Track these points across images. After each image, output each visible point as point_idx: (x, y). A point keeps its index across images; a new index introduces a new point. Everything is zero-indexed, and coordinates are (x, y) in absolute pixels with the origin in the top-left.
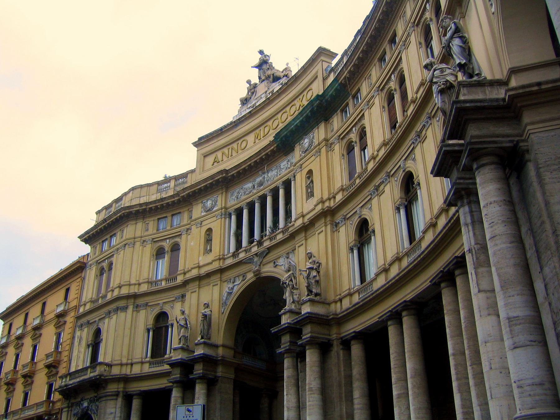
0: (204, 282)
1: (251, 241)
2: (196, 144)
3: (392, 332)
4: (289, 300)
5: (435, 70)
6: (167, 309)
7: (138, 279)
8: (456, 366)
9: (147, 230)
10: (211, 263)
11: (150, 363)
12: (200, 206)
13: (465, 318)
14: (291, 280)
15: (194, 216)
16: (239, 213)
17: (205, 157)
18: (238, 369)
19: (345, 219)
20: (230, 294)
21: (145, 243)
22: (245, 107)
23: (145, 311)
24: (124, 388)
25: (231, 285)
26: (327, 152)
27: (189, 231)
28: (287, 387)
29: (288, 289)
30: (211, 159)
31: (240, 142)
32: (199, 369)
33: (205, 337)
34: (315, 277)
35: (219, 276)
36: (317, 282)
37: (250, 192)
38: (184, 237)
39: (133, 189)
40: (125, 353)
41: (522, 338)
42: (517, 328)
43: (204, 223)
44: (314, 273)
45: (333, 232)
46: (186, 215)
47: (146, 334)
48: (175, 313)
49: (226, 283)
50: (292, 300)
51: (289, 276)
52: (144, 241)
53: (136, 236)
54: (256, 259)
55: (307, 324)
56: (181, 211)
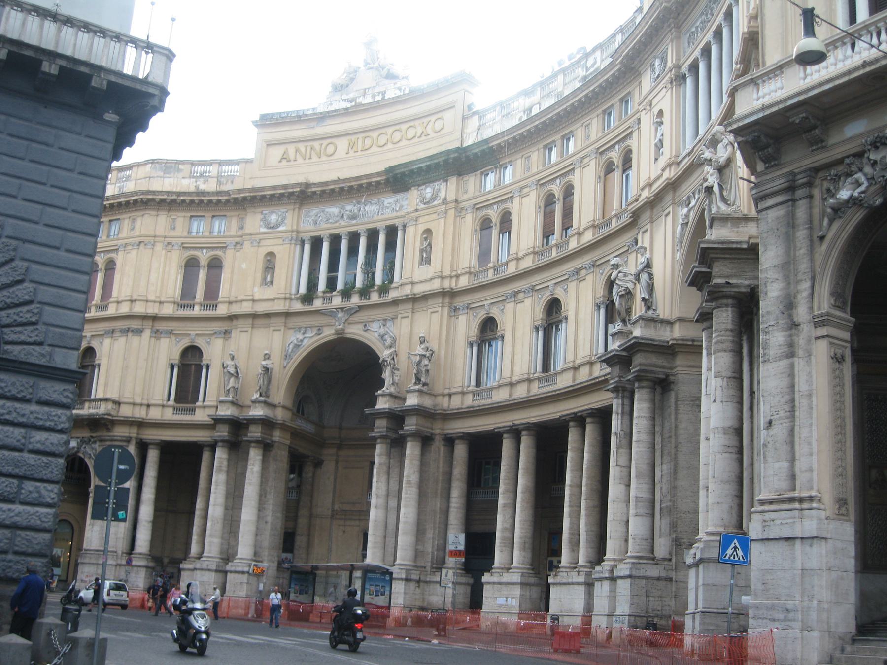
0: (259, 322)
1: (331, 283)
2: (256, 124)
3: (507, 446)
5: (620, 272)
6: (200, 343)
7: (158, 295)
8: (571, 495)
9: (174, 228)
10: (273, 300)
12: (259, 217)
13: (588, 460)
15: (248, 229)
16: (316, 244)
17: (268, 145)
18: (295, 434)
19: (468, 307)
20: (297, 346)
21: (170, 247)
22: (337, 97)
23: (168, 340)
24: (138, 434)
25: (300, 337)
26: (456, 217)
27: (238, 247)
28: (378, 474)
29: (389, 368)
30: (277, 152)
31: (325, 142)
32: (255, 432)
33: (264, 394)
34: (426, 365)
35: (282, 320)
36: (427, 371)
37: (336, 222)
38: (230, 253)
39: (153, 162)
40: (138, 390)
41: (642, 511)
42: (640, 504)
43: (263, 243)
44: (426, 361)
46: (234, 222)
47: (169, 371)
48: (215, 353)
49: (291, 331)
51: (391, 354)
52: (169, 244)
53: (158, 234)
54: (340, 315)
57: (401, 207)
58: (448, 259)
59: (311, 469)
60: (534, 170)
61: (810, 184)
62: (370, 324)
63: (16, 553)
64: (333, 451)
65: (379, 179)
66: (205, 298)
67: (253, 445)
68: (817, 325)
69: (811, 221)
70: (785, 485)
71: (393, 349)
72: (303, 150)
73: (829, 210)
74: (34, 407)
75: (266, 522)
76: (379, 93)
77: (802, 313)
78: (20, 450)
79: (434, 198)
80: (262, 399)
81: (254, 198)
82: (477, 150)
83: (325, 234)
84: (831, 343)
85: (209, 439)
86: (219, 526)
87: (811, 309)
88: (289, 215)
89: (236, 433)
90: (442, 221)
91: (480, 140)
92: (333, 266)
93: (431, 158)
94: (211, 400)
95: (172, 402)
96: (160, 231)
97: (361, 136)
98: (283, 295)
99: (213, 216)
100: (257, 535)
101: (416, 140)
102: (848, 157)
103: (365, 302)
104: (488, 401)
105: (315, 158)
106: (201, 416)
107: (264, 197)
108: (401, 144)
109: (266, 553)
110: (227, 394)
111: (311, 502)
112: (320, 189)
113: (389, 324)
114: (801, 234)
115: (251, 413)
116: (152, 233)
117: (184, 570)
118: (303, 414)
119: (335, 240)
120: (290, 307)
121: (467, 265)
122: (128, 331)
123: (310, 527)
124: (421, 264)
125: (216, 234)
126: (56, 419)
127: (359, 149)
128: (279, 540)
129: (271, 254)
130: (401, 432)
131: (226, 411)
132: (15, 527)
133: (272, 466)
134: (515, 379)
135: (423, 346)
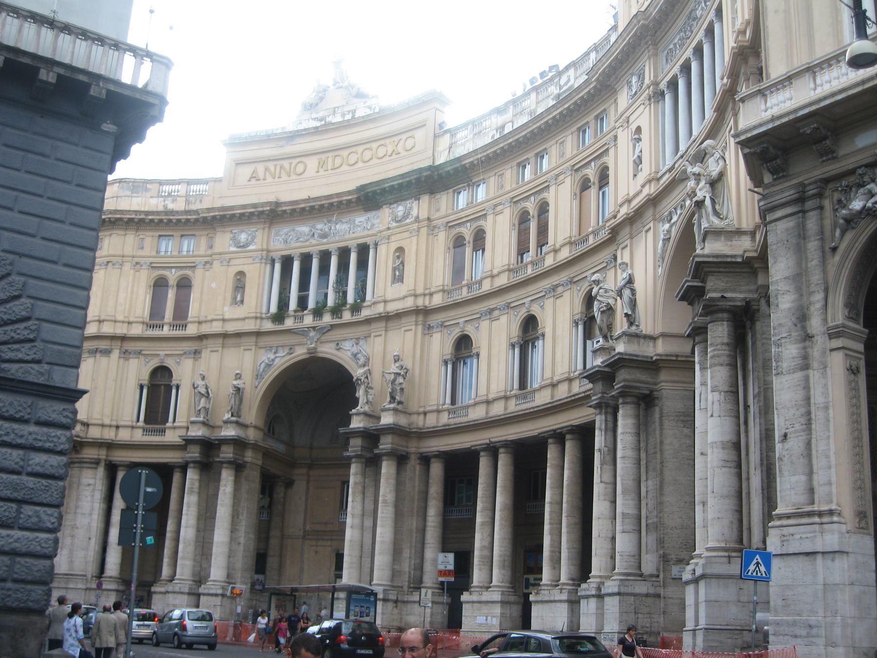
1: (303, 302)
4: (362, 400)
5: (600, 288)
6: (170, 363)
7: (126, 315)
8: (551, 512)
9: (142, 248)
10: (244, 319)
11: (144, 429)
12: (228, 236)
13: (568, 477)
14: (367, 377)
15: (218, 248)
16: (287, 262)
17: (237, 164)
18: (267, 454)
19: (442, 325)
20: (269, 366)
21: (138, 267)
23: (137, 360)
24: (107, 456)
25: (272, 356)
26: (428, 235)
27: (208, 266)
28: (353, 493)
29: (363, 387)
30: (247, 171)
31: (295, 161)
32: (227, 453)
34: (401, 384)
35: (253, 339)
36: (402, 389)
38: (199, 272)
40: (107, 411)
41: (628, 527)
42: (627, 521)
43: (233, 262)
44: (400, 380)
45: (424, 334)
46: (203, 241)
48: (185, 373)
49: (262, 351)
50: (365, 401)
51: (365, 373)
52: (137, 263)
53: (126, 253)
54: (312, 334)
55: (388, 434)
56: (197, 233)
57: (373, 225)
58: (421, 278)
59: (283, 489)
60: (508, 188)
61: (820, 195)
62: (343, 343)
63: (15, 581)
64: (304, 471)
65: (350, 197)
66: (175, 318)
67: (225, 465)
68: (831, 337)
69: (822, 232)
70: (802, 498)
71: (366, 368)
72: (272, 169)
73: (841, 221)
74: (32, 428)
75: (239, 544)
76: (349, 112)
77: (815, 324)
78: (18, 473)
79: (406, 216)
80: (234, 419)
81: (223, 217)
82: (449, 168)
83: (296, 253)
84: (846, 355)
85: (180, 460)
86: (191, 549)
87: (825, 320)
88: (259, 234)
89: (208, 454)
90: (414, 239)
91: (452, 158)
92: (304, 285)
93: (402, 176)
94: (181, 420)
95: (141, 423)
96: (128, 251)
97: (331, 154)
98: (254, 315)
99: (182, 236)
100: (229, 557)
101: (386, 158)
102: (860, 167)
103: (337, 321)
104: (465, 419)
105: (284, 177)
106: (172, 437)
107: (233, 216)
108: (371, 163)
109: (240, 575)
110: (198, 415)
111: (283, 522)
112: (290, 207)
113: (361, 343)
114: (813, 245)
115: (223, 434)
116: (120, 253)
117: (155, 593)
118: (273, 433)
119: (306, 259)
120: (261, 326)
121: (440, 282)
122: (96, 352)
123: (282, 547)
124: (393, 282)
125: (185, 253)
126: (55, 440)
127: (330, 167)
128: (251, 562)
129: (241, 274)
130: (376, 451)
131: (197, 432)
132: (14, 553)
133: (245, 487)
134: (491, 396)
135: (397, 365)
